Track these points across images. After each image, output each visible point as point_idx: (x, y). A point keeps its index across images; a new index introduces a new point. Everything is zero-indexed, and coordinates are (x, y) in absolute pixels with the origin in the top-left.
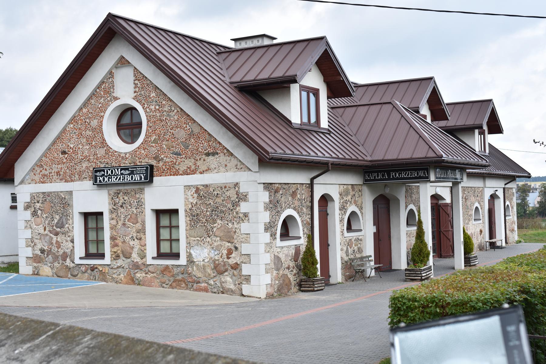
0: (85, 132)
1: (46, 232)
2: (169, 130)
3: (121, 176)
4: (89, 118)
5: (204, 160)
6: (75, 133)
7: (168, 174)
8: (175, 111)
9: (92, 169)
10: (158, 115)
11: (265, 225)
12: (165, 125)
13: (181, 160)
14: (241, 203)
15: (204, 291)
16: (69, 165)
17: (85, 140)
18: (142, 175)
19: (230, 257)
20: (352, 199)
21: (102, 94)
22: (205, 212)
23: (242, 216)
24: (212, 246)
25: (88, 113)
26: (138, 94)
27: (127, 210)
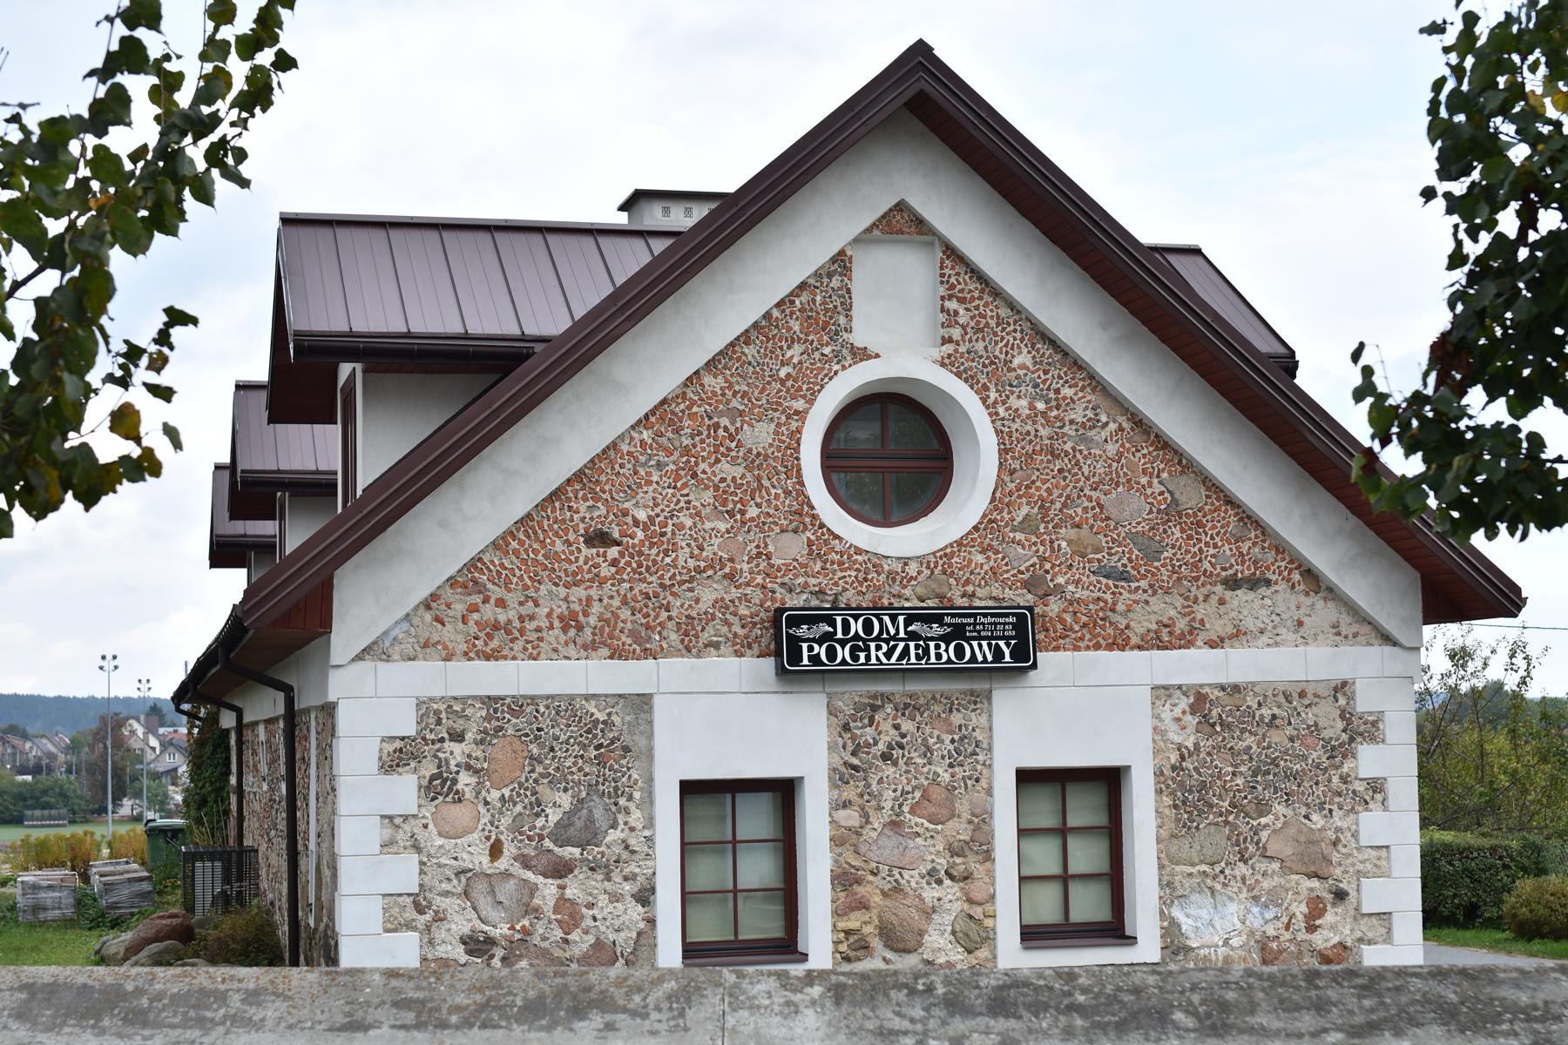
0: (711, 466)
3: (912, 644)
5: (1222, 602)
7: (1086, 643)
8: (1113, 426)
10: (1044, 432)
12: (1069, 471)
13: (1133, 597)
16: (631, 589)
17: (708, 496)
21: (797, 328)
22: (1228, 778)
23: (1362, 789)
24: (1256, 892)
25: (729, 393)
26: (962, 349)
27: (907, 772)
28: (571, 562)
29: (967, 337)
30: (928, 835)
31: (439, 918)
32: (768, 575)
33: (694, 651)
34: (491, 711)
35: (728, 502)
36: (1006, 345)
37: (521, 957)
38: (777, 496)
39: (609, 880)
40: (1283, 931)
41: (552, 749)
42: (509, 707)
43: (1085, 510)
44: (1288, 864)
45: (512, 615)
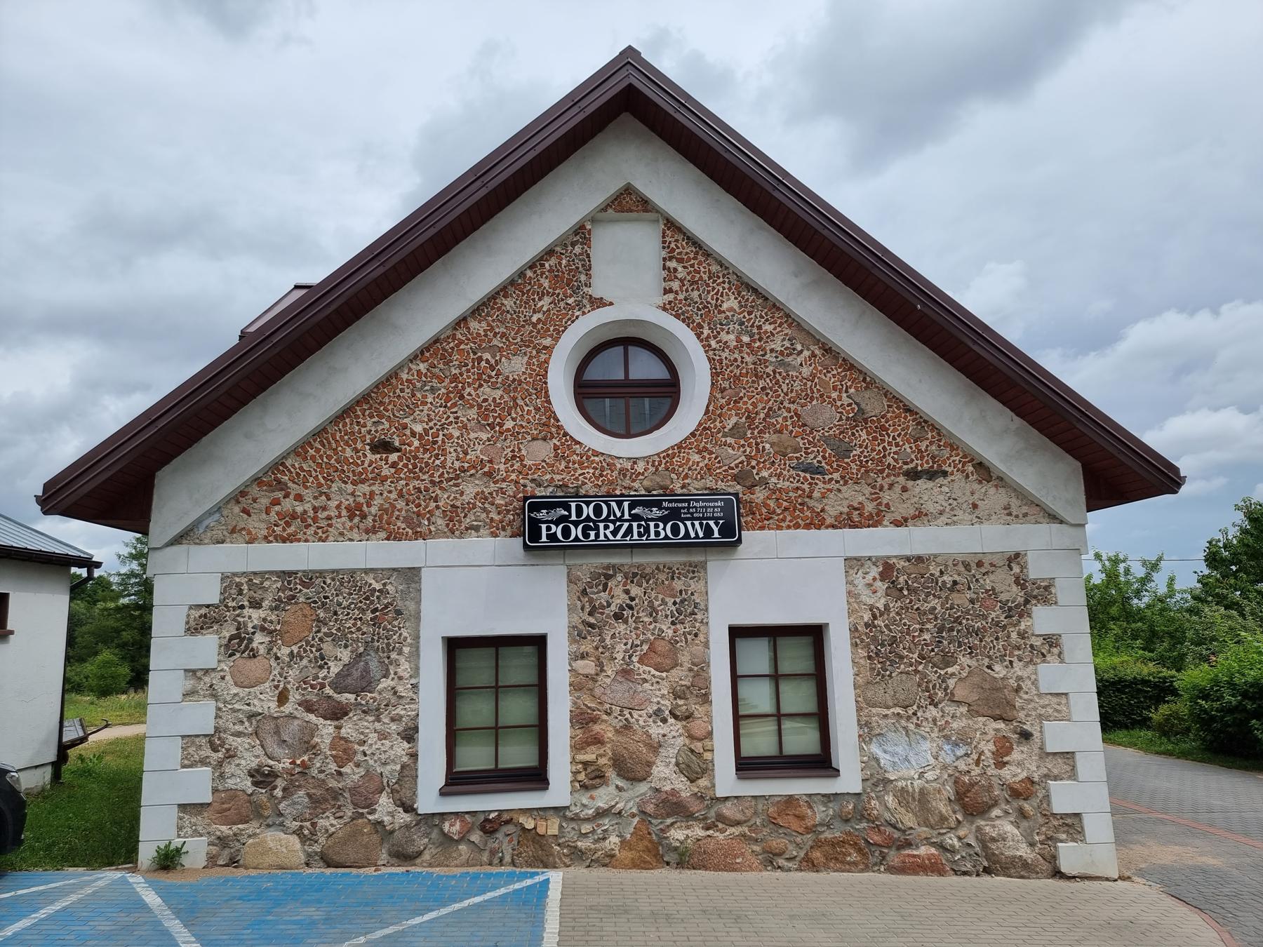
0: (476, 389)
2: (786, 404)
3: (635, 524)
5: (904, 489)
8: (806, 353)
10: (748, 359)
13: (828, 486)
15: (932, 872)
16: (407, 485)
17: (473, 413)
19: (1007, 763)
21: (546, 284)
22: (916, 634)
23: (1038, 643)
26: (681, 297)
27: (637, 628)
28: (358, 465)
29: (684, 288)
30: (654, 680)
31: (231, 755)
32: (520, 473)
33: (457, 533)
34: (286, 583)
35: (489, 418)
36: (717, 294)
37: (299, 786)
38: (529, 412)
39: (379, 720)
40: (973, 767)
41: (335, 613)
42: (301, 579)
43: (785, 419)
44: (975, 708)
45: (308, 507)
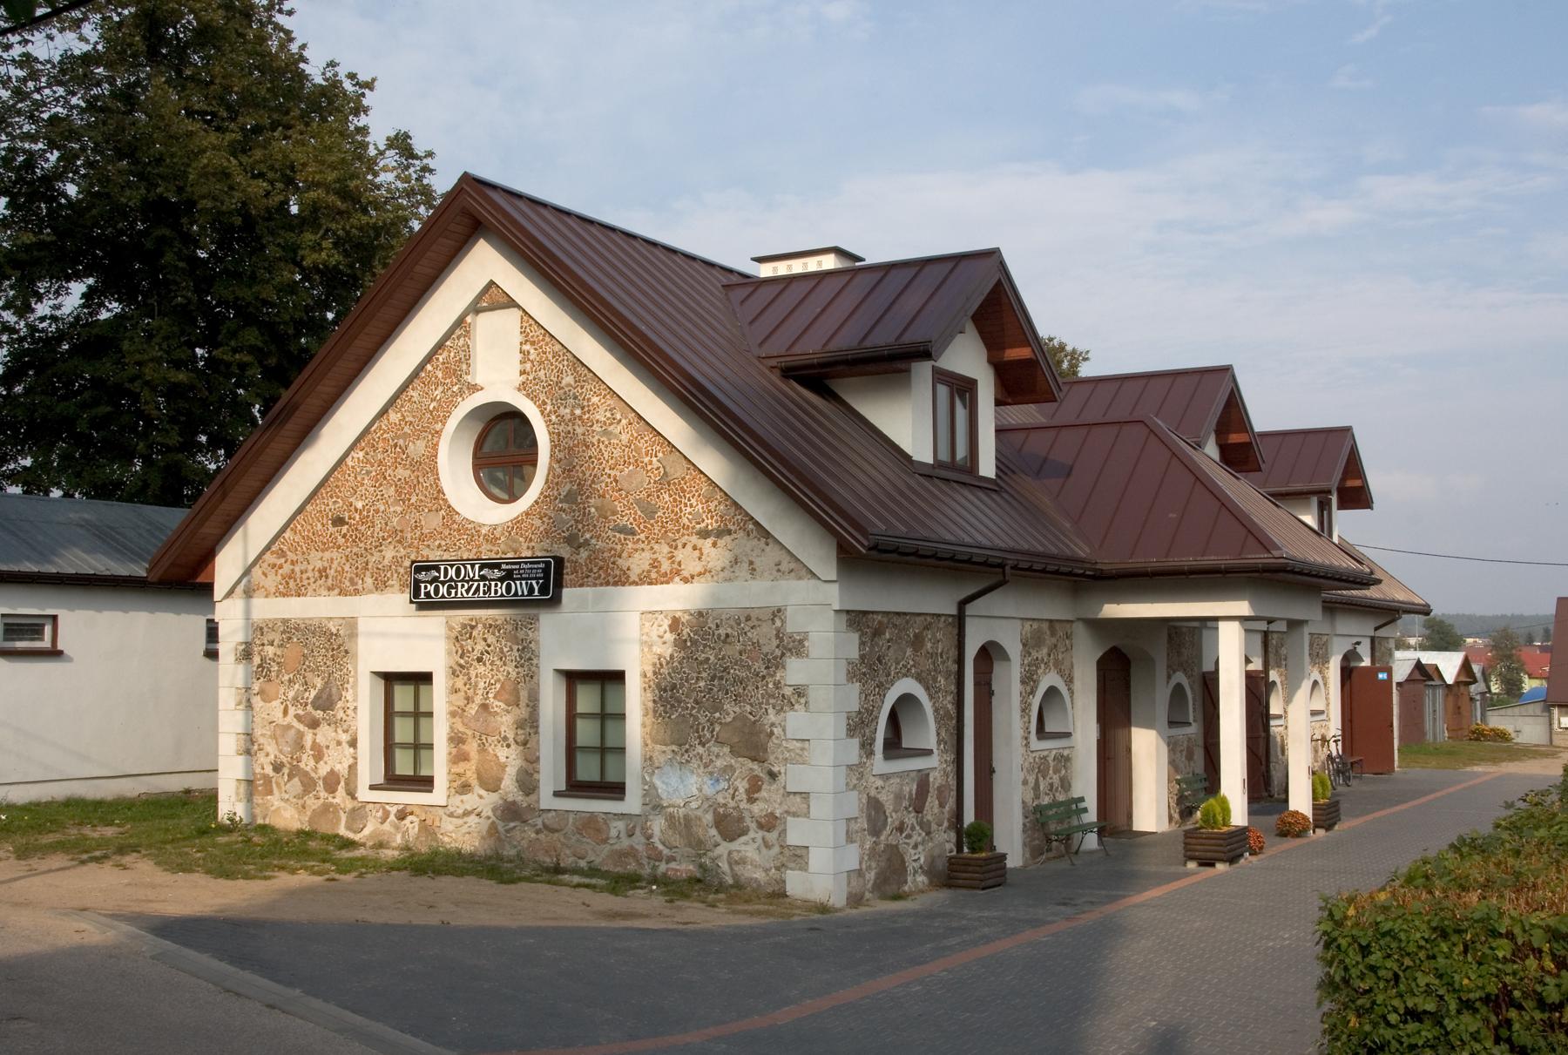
1: (290, 719)
4: (405, 436)
6: (368, 473)
8: (624, 422)
9: (407, 563)
10: (579, 430)
11: (848, 719)
13: (635, 547)
14: (788, 660)
18: (534, 582)
20: (1049, 655)
21: (440, 375)
23: (789, 693)
26: (531, 377)
27: (492, 670)
